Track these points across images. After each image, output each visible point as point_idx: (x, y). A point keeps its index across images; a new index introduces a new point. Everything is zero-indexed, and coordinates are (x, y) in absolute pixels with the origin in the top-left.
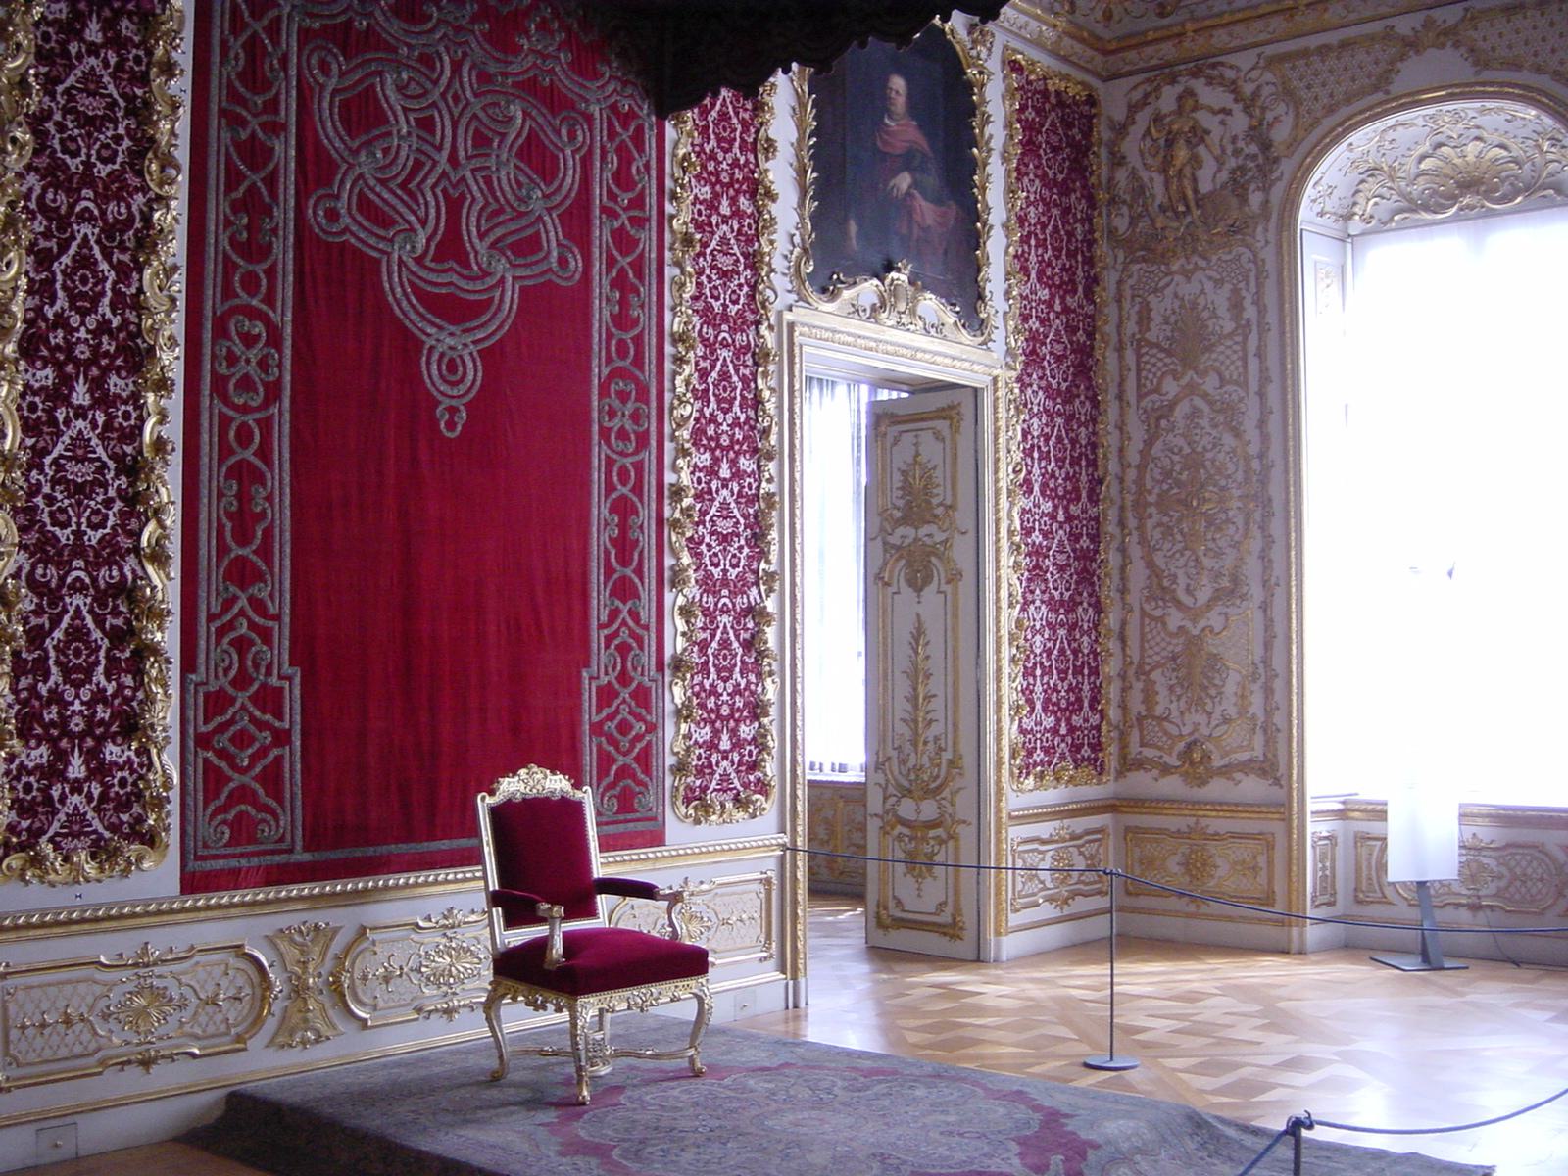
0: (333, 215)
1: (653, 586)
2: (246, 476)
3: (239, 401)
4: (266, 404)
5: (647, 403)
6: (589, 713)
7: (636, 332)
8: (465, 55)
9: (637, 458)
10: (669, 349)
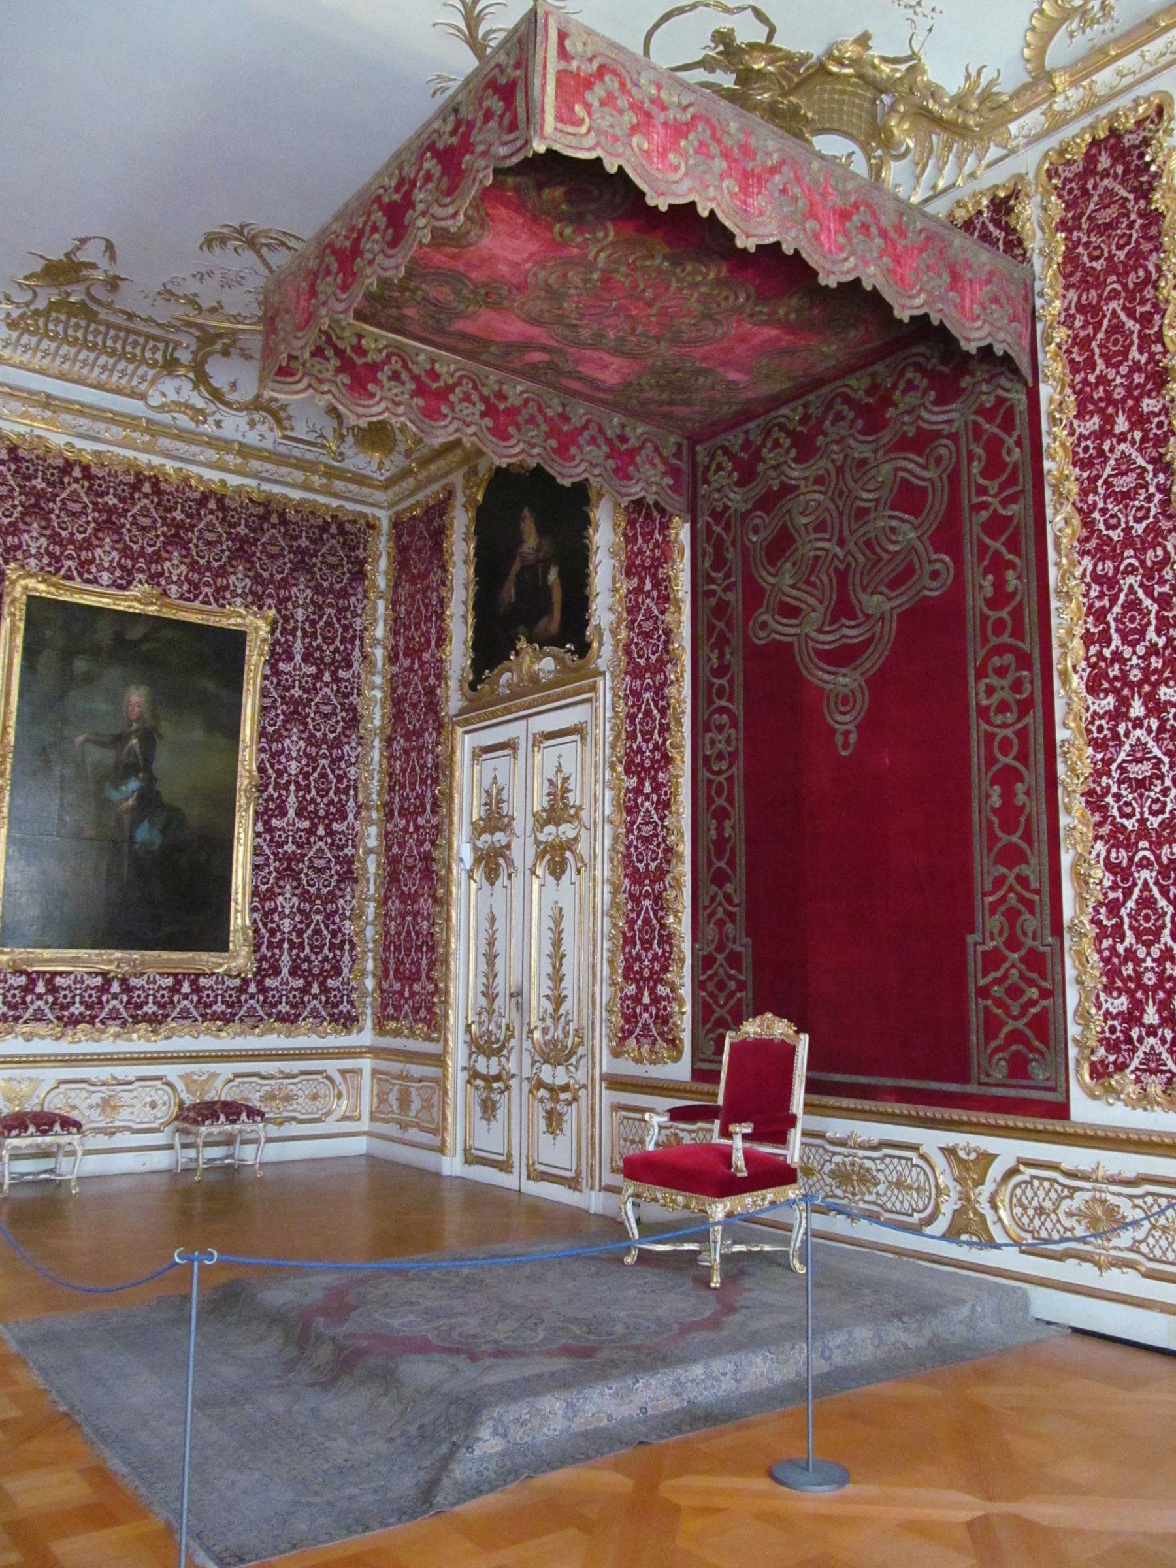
0: (764, 626)
1: (1045, 848)
2: (721, 815)
3: (715, 768)
4: (730, 766)
5: (1029, 668)
6: (976, 979)
7: (1014, 604)
8: (846, 457)
9: (1019, 725)
10: (1054, 604)
